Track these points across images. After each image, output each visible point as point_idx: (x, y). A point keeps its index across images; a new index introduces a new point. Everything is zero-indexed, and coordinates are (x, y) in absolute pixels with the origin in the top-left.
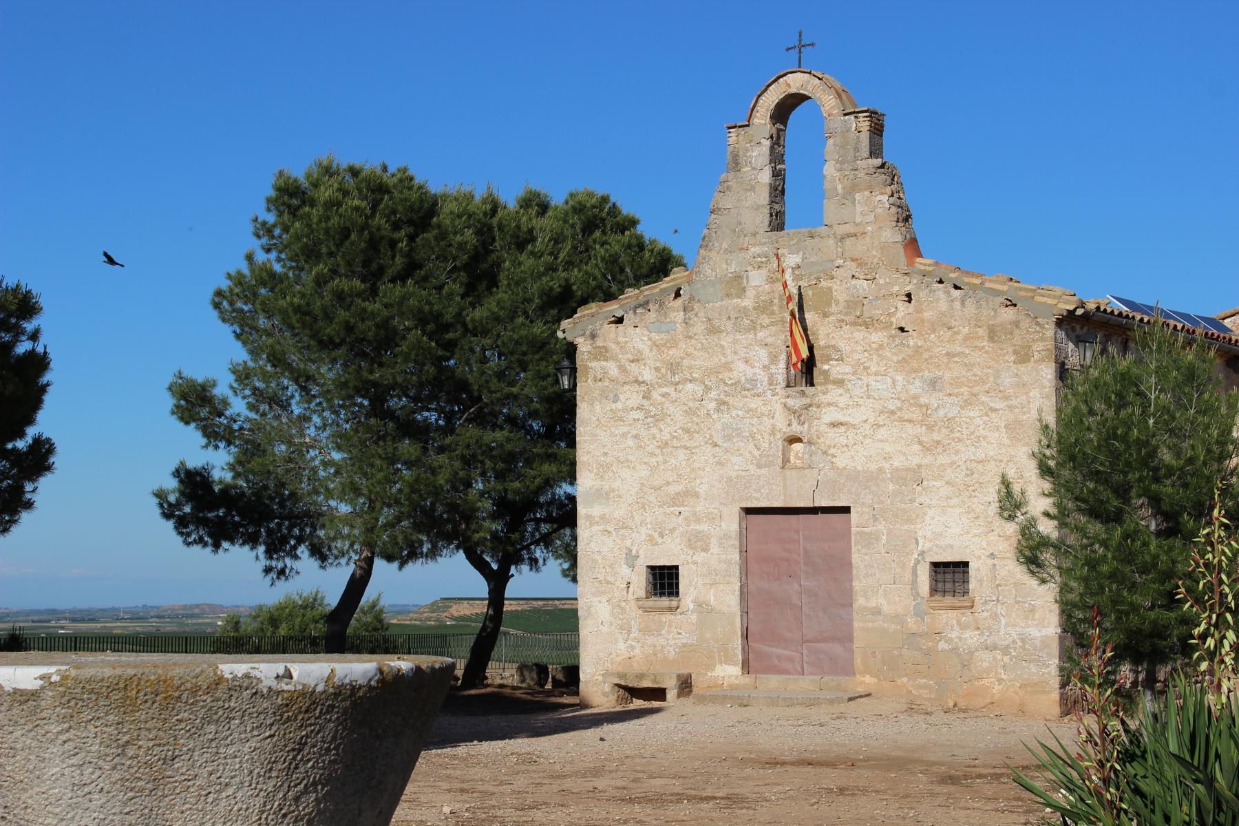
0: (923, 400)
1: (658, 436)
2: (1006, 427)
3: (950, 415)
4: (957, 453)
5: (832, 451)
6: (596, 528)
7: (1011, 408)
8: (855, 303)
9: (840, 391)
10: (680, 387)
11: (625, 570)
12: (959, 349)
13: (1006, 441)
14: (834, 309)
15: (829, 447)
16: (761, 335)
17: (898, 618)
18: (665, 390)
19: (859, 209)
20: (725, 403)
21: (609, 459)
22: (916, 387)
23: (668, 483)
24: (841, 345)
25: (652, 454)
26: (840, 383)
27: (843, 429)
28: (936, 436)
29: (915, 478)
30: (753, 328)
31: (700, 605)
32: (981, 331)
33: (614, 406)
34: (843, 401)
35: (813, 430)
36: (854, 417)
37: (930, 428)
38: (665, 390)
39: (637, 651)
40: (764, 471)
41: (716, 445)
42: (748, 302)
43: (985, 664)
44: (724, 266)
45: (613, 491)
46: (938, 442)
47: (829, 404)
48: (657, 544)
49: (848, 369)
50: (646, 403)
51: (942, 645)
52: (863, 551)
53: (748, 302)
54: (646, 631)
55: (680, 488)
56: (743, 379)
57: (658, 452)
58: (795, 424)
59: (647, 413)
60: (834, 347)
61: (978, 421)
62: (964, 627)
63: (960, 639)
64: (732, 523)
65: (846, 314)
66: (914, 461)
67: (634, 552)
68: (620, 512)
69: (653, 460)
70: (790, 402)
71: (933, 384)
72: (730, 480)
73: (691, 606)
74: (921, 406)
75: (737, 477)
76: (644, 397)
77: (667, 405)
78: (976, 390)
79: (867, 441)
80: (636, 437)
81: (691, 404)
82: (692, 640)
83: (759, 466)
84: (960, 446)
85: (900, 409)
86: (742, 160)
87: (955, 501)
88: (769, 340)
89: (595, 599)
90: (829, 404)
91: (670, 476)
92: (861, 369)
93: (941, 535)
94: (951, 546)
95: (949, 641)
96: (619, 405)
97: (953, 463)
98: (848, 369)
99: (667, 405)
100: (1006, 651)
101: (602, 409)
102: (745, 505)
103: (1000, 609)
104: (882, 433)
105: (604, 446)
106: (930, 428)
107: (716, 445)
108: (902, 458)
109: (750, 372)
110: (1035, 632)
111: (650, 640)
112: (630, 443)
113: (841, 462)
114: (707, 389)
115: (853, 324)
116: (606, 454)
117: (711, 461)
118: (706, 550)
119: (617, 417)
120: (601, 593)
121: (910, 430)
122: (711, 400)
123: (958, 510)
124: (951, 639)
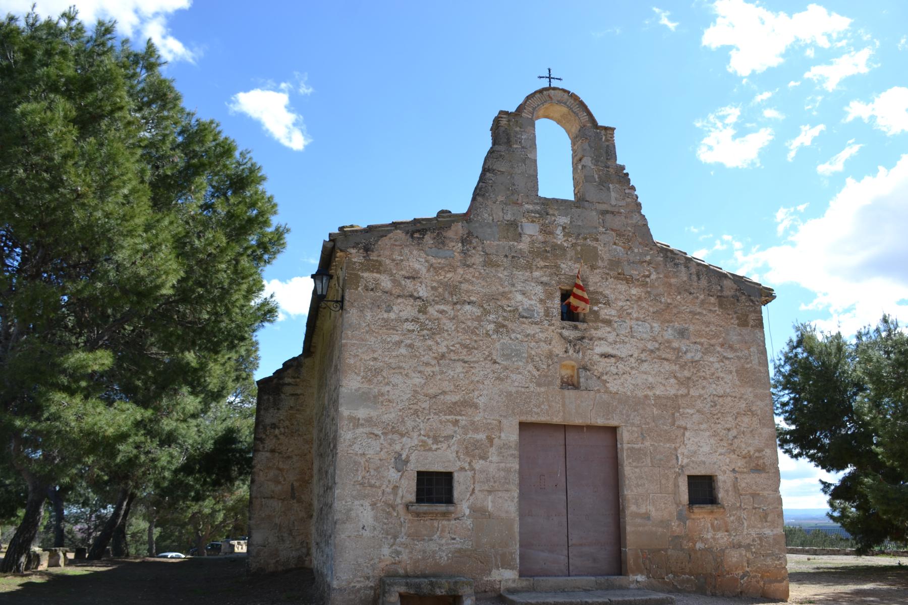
0: (675, 345)
1: (434, 348)
2: (737, 371)
3: (696, 358)
4: (704, 388)
5: (605, 377)
6: (361, 430)
7: (739, 358)
8: (615, 263)
9: (609, 329)
10: (458, 307)
11: (393, 475)
12: (699, 310)
13: (738, 383)
14: (600, 263)
15: (602, 374)
16: (537, 274)
17: (664, 523)
18: (442, 307)
19: (613, 194)
20: (504, 326)
21: (379, 364)
22: (669, 334)
23: (444, 393)
24: (607, 292)
25: (427, 364)
26: (608, 322)
27: (613, 360)
28: (687, 373)
29: (671, 405)
30: (529, 267)
31: (474, 509)
32: (712, 300)
33: (386, 315)
34: (611, 337)
35: (587, 359)
36: (622, 351)
37: (682, 367)
38: (442, 307)
39: (404, 557)
40: (543, 389)
41: (495, 362)
42: (523, 246)
43: (734, 560)
44: (501, 214)
45: (383, 395)
46: (689, 378)
47: (600, 339)
48: (430, 450)
49: (613, 312)
50: (422, 317)
51: (699, 545)
52: (634, 464)
53: (523, 246)
54: (415, 536)
55: (456, 398)
56: (521, 309)
57: (434, 362)
58: (571, 352)
59: (423, 326)
60: (601, 293)
61: (717, 365)
62: (715, 529)
63: (713, 538)
64: (512, 435)
65: (609, 269)
66: (672, 392)
67: (404, 457)
68: (391, 416)
69: (429, 370)
70: (566, 333)
71: (682, 333)
72: (509, 394)
73: (467, 512)
74: (674, 349)
75: (517, 392)
76: (419, 311)
77: (444, 321)
78: (713, 341)
79: (634, 372)
80: (411, 346)
81: (469, 323)
82: (468, 545)
83: (539, 385)
84: (705, 383)
85: (658, 349)
86: (513, 139)
87: (703, 426)
88: (545, 279)
89: (356, 502)
90: (600, 339)
91: (447, 386)
92: (623, 314)
93: (695, 452)
94: (704, 463)
95: (702, 539)
96: (392, 316)
97: (700, 396)
98: (613, 312)
99: (444, 321)
100: (748, 547)
101: (373, 316)
102: (524, 419)
103: (744, 515)
104: (645, 366)
105: (374, 351)
106: (682, 367)
107: (495, 362)
108: (662, 388)
109: (527, 303)
110: (767, 532)
111: (419, 546)
112: (403, 351)
113: (613, 386)
114: (487, 312)
115: (616, 278)
116: (375, 359)
117: (491, 375)
118: (484, 457)
119: (388, 325)
120: (365, 497)
121: (667, 366)
122: (490, 322)
123: (708, 434)
124: (707, 539)
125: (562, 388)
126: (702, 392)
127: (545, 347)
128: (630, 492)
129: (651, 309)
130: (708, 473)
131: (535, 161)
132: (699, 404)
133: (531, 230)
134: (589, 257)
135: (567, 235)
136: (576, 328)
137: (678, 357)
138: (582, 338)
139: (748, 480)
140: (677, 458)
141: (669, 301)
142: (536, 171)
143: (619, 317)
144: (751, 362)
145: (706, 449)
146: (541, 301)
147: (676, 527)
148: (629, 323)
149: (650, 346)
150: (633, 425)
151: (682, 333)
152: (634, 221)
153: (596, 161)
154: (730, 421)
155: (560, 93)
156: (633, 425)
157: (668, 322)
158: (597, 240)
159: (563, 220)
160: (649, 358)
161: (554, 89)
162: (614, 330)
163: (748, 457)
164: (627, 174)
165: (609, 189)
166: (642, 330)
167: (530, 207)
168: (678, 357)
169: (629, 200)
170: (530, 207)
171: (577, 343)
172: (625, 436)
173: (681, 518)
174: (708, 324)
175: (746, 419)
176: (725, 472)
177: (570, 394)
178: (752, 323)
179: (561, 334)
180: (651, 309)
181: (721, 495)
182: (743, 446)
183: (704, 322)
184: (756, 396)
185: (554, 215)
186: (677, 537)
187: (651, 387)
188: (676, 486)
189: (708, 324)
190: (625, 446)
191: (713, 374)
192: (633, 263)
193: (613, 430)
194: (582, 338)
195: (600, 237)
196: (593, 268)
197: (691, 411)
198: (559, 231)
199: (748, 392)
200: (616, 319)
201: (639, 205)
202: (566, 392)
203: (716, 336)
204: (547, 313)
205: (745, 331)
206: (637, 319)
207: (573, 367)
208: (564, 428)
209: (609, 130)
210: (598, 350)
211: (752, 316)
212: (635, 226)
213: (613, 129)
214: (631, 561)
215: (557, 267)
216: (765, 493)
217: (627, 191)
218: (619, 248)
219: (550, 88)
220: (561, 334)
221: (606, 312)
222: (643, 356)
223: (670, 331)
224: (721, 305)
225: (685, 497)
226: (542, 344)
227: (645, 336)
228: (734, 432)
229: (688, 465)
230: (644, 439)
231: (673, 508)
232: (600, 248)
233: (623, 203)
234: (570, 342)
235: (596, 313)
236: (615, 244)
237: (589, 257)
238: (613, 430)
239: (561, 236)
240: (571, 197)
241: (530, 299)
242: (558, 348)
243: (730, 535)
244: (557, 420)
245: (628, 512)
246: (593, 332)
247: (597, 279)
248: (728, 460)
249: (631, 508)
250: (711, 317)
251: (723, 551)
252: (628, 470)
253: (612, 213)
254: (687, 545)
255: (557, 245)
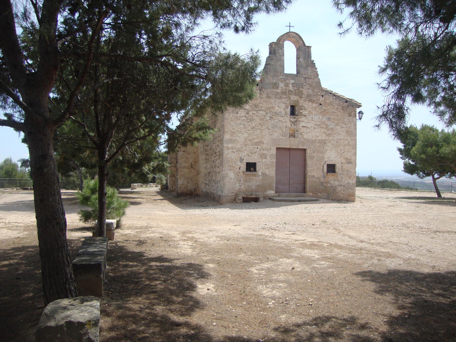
0: (326, 123)
2: (346, 131)
3: (333, 127)
4: (334, 137)
5: (303, 134)
7: (347, 127)
8: (309, 96)
9: (305, 118)
12: (335, 111)
13: (346, 135)
14: (304, 96)
15: (302, 132)
16: (283, 100)
17: (319, 178)
19: (309, 71)
22: (324, 119)
24: (305, 106)
26: (305, 116)
27: (306, 128)
28: (329, 132)
29: (323, 142)
30: (281, 98)
32: (340, 107)
34: (306, 121)
35: (297, 128)
36: (309, 125)
37: (328, 130)
42: (279, 91)
43: (339, 190)
44: (272, 80)
46: (330, 134)
47: (302, 121)
49: (307, 113)
51: (329, 185)
53: (279, 91)
58: (293, 125)
60: (303, 106)
61: (339, 129)
62: (334, 180)
63: (334, 183)
65: (307, 98)
66: (324, 138)
70: (291, 119)
71: (329, 119)
78: (339, 122)
84: (335, 135)
85: (321, 124)
86: (276, 52)
87: (334, 149)
88: (285, 102)
90: (302, 121)
92: (310, 113)
93: (330, 157)
94: (332, 160)
95: (330, 184)
97: (333, 139)
98: (307, 113)
100: (344, 186)
103: (344, 176)
104: (316, 130)
106: (328, 130)
108: (321, 137)
110: (350, 182)
115: (309, 101)
121: (323, 130)
123: (334, 151)
124: (331, 183)
125: (290, 137)
126: (334, 138)
127: (285, 124)
128: (309, 169)
129: (319, 111)
130: (334, 164)
131: (284, 60)
132: (332, 142)
133: (282, 85)
134: (300, 94)
135: (293, 87)
136: (295, 118)
137: (327, 127)
138: (297, 121)
139: (346, 166)
140: (324, 159)
141: (325, 108)
142: (284, 64)
143: (309, 114)
144: (351, 128)
145: (334, 156)
146: (284, 109)
147: (322, 180)
148: (312, 116)
149: (318, 123)
150: (311, 148)
151: (329, 119)
152: (316, 81)
153: (304, 59)
154: (342, 147)
155: (293, 34)
156: (311, 148)
157: (324, 115)
158: (303, 88)
159: (292, 81)
160: (317, 127)
161: (291, 32)
162: (307, 118)
163: (347, 159)
164: (315, 63)
165: (308, 69)
166: (316, 118)
167: (281, 77)
168: (327, 127)
169: (314, 73)
170: (281, 77)
171: (294, 123)
172: (308, 152)
173: (324, 177)
174: (338, 116)
175: (347, 147)
176: (339, 163)
177: (292, 139)
178: (352, 115)
179: (290, 120)
180: (319, 111)
181: (337, 170)
182: (346, 155)
183: (336, 115)
184: (351, 139)
185: (289, 80)
186: (323, 182)
187: (317, 137)
188: (323, 167)
189: (338, 116)
190: (308, 155)
191: (338, 132)
192: (315, 95)
193: (305, 150)
194: (297, 121)
195: (304, 87)
196: (301, 97)
197: (329, 144)
198: (291, 85)
199: (349, 138)
200: (307, 115)
201: (318, 75)
202: (291, 138)
203: (340, 120)
204: (286, 113)
205: (350, 118)
206: (315, 115)
207: (293, 130)
208: (289, 149)
209: (309, 47)
210: (301, 125)
211: (353, 113)
212: (316, 82)
213: (311, 47)
214: (308, 189)
215: (290, 98)
216: (351, 170)
217: (314, 70)
218: (310, 91)
219: (290, 32)
220: (290, 120)
221: (304, 112)
222: (315, 127)
223: (325, 118)
224: (343, 109)
225: (325, 170)
226: (284, 123)
227: (317, 120)
228: (343, 151)
229: (327, 161)
230: (314, 152)
231: (322, 174)
232: (304, 91)
233: (312, 74)
234: (293, 122)
235: (301, 113)
236: (308, 89)
237: (300, 94)
238: (305, 150)
239: (291, 87)
240: (295, 72)
241: (281, 109)
242: (289, 124)
243: (339, 182)
244: (288, 147)
245: (308, 175)
246: (300, 119)
247: (302, 101)
248: (340, 160)
249: (309, 174)
250: (339, 114)
251: (336, 187)
252: (309, 162)
253: (309, 78)
254: (325, 185)
255: (290, 90)
